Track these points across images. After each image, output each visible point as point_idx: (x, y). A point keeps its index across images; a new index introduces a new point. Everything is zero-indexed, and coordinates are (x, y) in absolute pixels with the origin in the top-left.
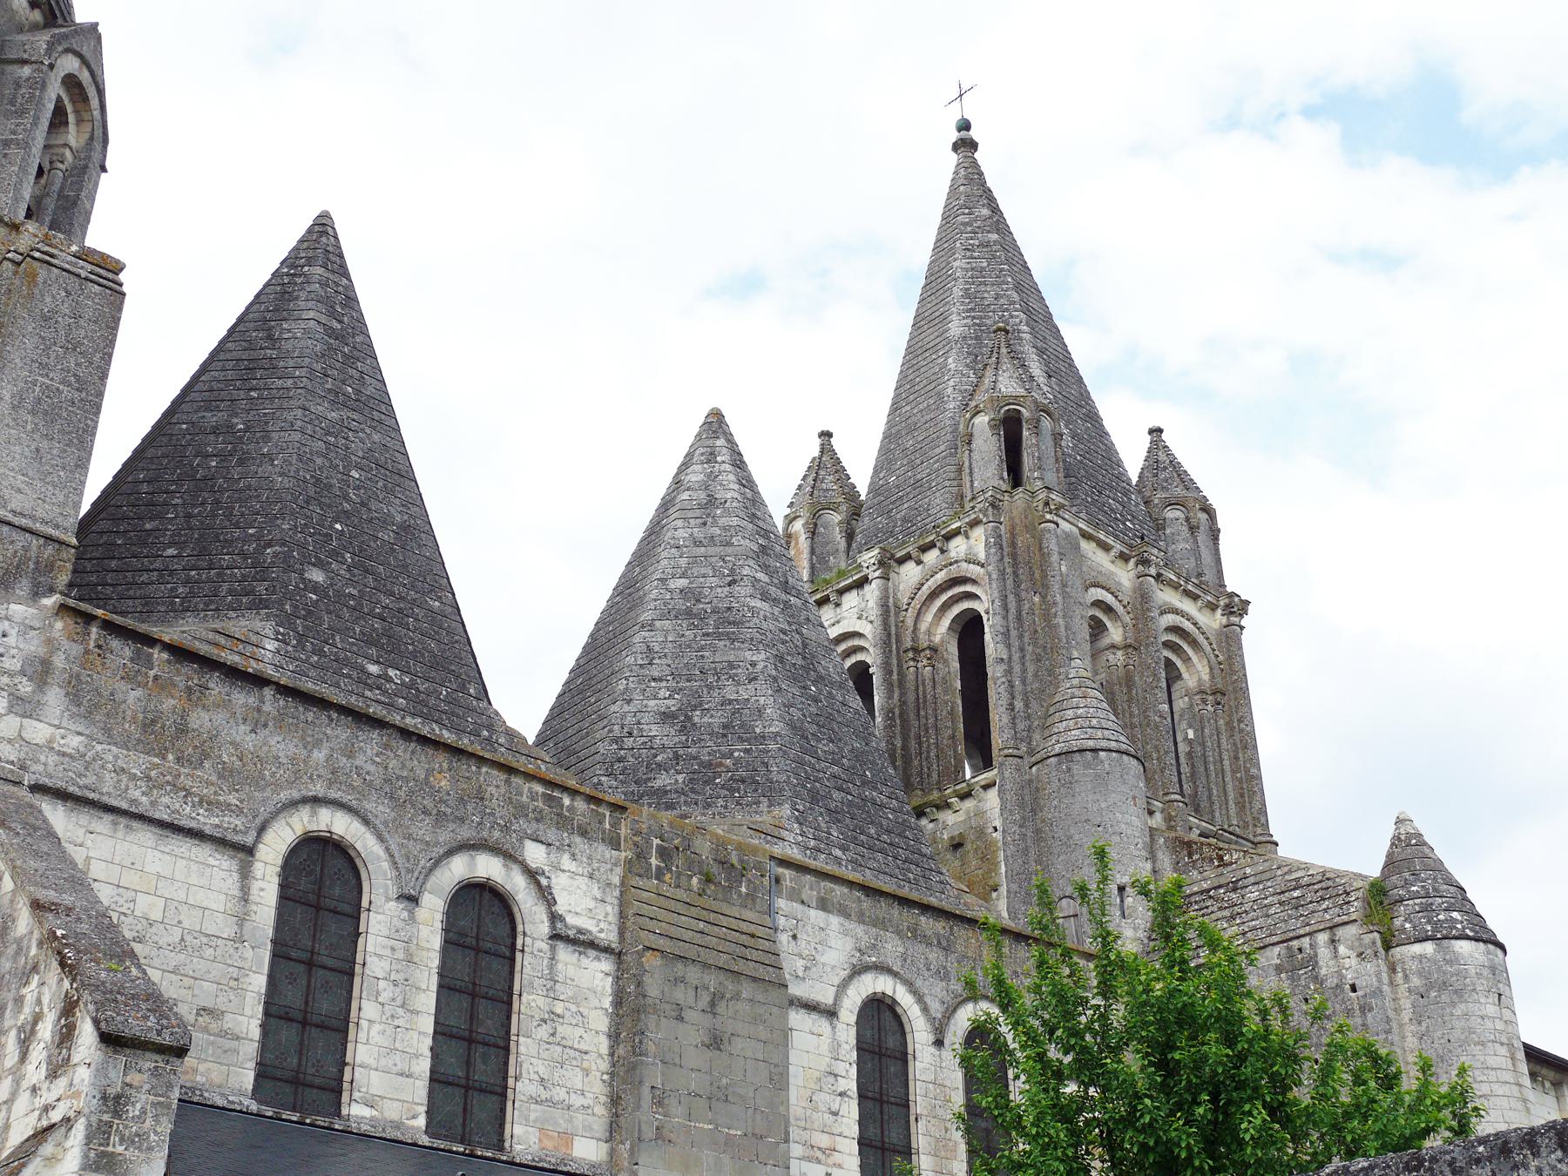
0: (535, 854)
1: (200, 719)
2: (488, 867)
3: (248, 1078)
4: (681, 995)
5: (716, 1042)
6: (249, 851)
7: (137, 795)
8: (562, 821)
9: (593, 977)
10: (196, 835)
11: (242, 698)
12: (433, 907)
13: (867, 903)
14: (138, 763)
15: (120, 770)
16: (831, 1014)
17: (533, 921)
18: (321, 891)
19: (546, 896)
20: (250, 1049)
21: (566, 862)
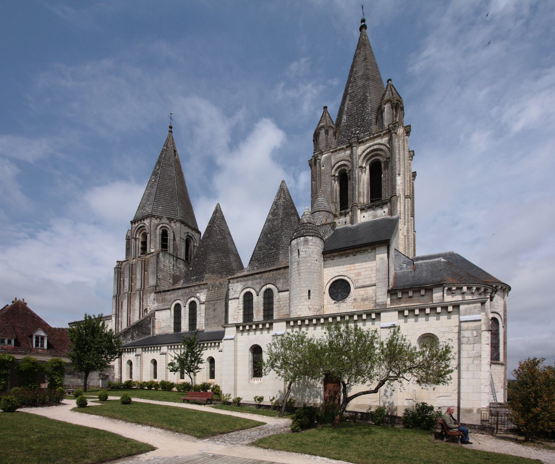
0: (198, 295)
1: (166, 297)
2: (193, 299)
3: (173, 331)
4: (210, 306)
5: (214, 310)
6: (170, 309)
7: (162, 308)
8: (201, 289)
9: (203, 307)
10: (166, 309)
11: (169, 293)
12: (187, 306)
13: (245, 278)
14: (161, 304)
15: (161, 306)
17: (198, 303)
18: (178, 308)
19: (199, 299)
20: (173, 328)
21: (202, 294)
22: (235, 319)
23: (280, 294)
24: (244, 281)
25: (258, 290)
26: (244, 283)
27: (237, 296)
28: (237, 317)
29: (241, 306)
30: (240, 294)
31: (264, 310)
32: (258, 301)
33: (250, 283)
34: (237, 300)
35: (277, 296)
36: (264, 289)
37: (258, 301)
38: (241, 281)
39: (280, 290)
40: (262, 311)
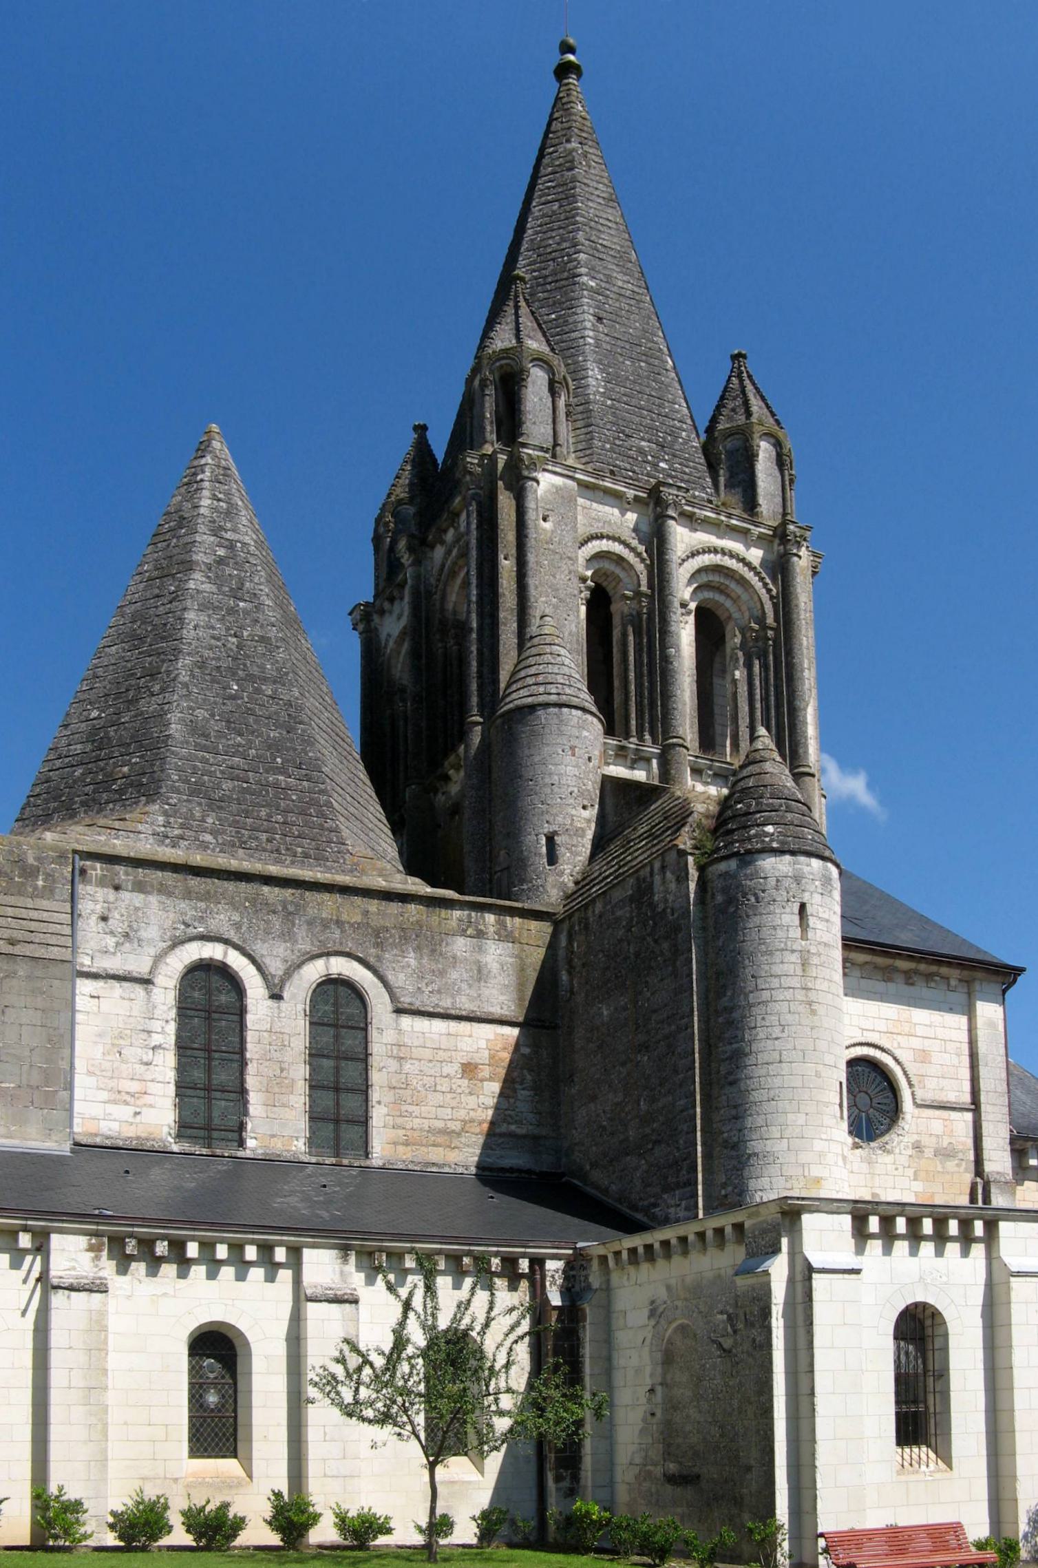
13: (194, 882)
16: (146, 982)
22: (119, 1097)
23: (406, 1021)
24: (188, 895)
25: (276, 967)
26: (183, 905)
27: (140, 966)
28: (134, 1087)
29: (167, 1033)
30: (159, 959)
31: (315, 1086)
32: (276, 1029)
33: (222, 920)
34: (139, 990)
35: (387, 1032)
36: (314, 971)
37: (276, 1029)
38: (163, 890)
39: (406, 1000)
40: (301, 1088)
